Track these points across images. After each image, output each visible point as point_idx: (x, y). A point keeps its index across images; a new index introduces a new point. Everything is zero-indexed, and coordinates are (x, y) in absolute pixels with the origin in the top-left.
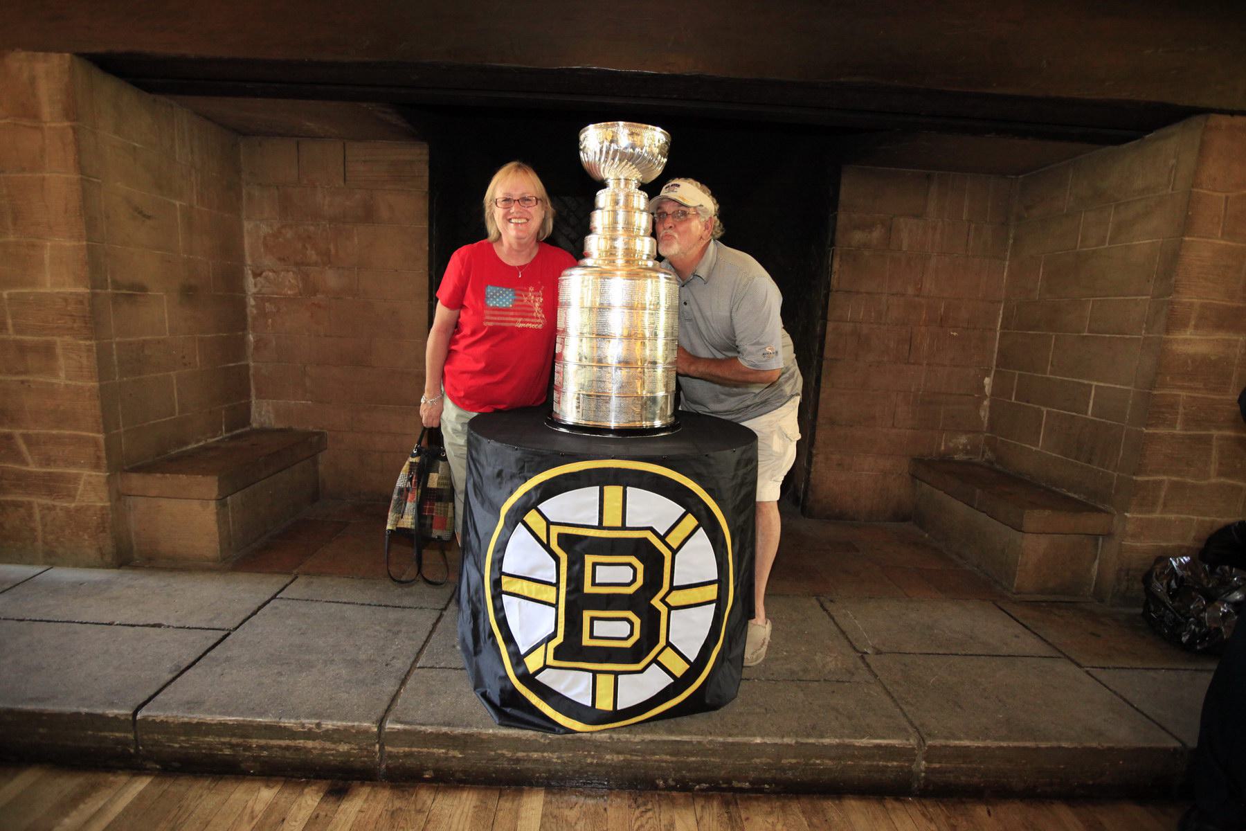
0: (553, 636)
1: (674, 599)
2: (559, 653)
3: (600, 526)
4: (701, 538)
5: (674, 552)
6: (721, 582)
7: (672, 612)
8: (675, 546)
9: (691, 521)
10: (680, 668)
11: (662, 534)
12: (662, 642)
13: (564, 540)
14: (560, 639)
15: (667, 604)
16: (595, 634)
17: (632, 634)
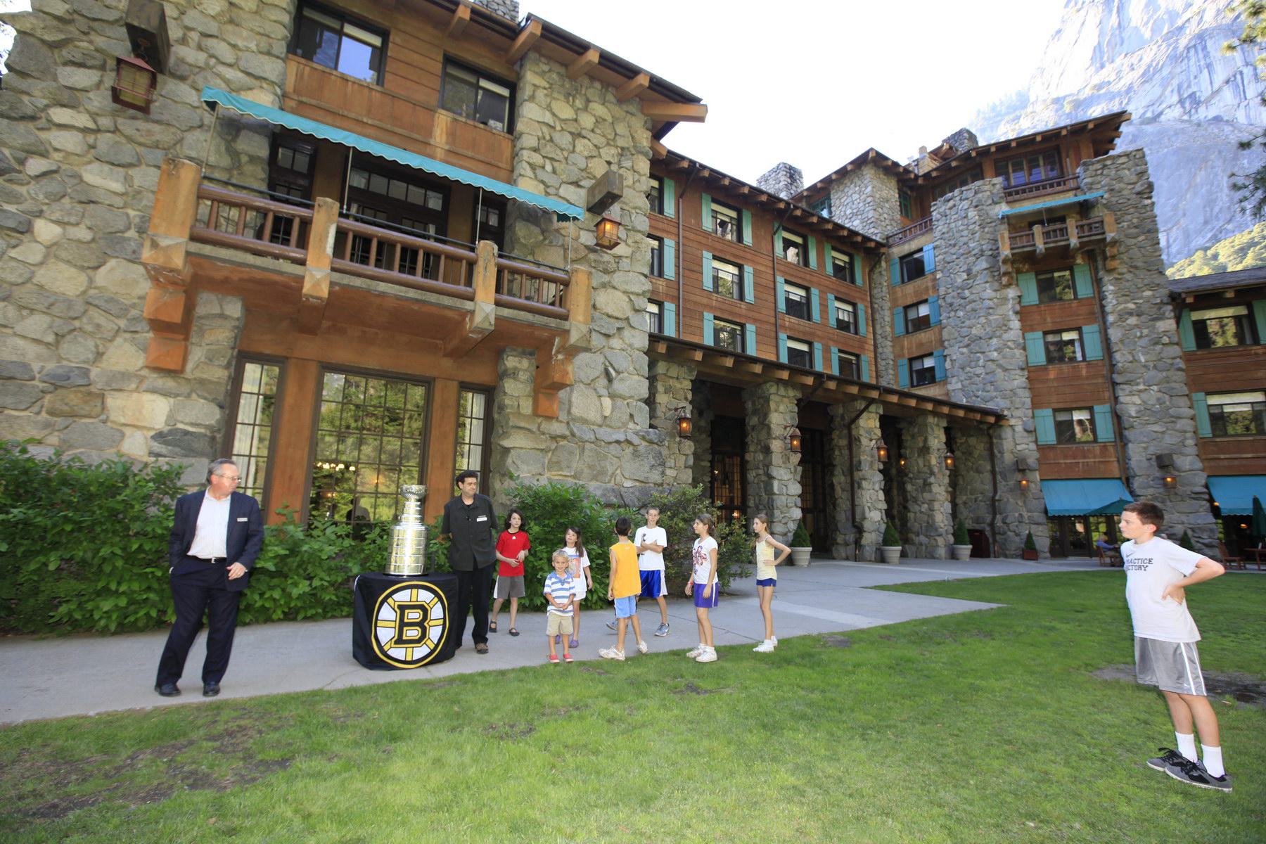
1: (431, 623)
2: (396, 643)
4: (439, 605)
6: (444, 618)
9: (436, 599)
10: (432, 646)
13: (400, 607)
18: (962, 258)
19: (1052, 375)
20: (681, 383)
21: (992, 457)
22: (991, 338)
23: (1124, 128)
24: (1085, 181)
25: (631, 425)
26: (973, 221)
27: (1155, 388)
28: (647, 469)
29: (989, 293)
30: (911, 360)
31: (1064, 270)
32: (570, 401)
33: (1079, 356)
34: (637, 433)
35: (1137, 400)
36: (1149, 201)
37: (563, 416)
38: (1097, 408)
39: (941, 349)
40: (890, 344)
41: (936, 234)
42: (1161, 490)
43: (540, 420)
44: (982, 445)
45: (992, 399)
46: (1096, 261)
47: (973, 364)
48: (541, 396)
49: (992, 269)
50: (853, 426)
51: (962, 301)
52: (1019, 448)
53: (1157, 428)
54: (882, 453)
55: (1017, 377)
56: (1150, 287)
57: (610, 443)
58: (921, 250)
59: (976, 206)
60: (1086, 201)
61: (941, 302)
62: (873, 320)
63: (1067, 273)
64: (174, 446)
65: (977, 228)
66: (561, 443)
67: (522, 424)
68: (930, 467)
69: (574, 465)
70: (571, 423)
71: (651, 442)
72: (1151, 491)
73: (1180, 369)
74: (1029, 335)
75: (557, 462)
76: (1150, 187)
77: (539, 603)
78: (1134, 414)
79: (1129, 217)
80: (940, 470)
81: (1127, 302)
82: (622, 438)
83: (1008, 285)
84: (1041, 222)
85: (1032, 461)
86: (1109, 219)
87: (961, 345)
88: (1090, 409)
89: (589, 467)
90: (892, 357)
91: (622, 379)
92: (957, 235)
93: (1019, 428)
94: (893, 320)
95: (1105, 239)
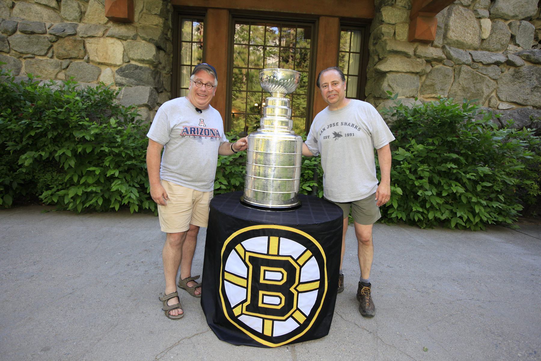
0: (245, 301)
1: (301, 288)
2: (248, 308)
3: (268, 254)
4: (314, 261)
5: (301, 267)
7: (299, 294)
8: (301, 264)
9: (309, 253)
10: (302, 319)
11: (295, 259)
12: (295, 308)
14: (248, 302)
15: (297, 290)
16: (264, 302)
17: (281, 303)
20: (533, 24)
25: (511, 47)
28: (528, 91)
32: (447, 25)
34: (519, 55)
37: (439, 41)
43: (416, 45)
48: (419, 20)
57: (489, 65)
64: (130, 78)
66: (436, 67)
67: (400, 48)
69: (448, 87)
70: (447, 47)
71: (536, 63)
75: (432, 85)
77: (416, 219)
82: (502, 59)
89: (464, 90)
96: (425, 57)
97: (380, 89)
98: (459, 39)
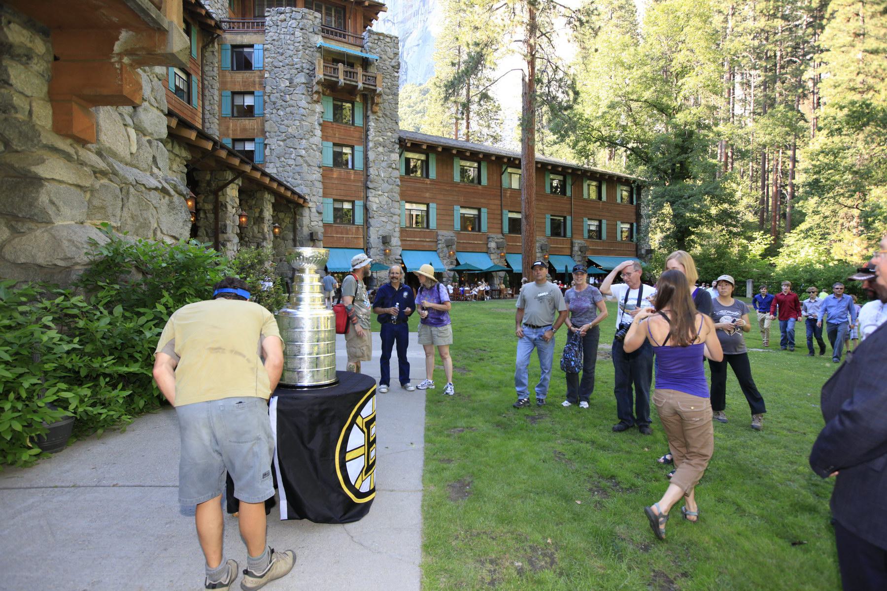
18: (287, 67)
19: (335, 175)
21: (294, 230)
22: (301, 139)
23: (381, 15)
24: (369, 44)
25: (155, 170)
26: (298, 40)
27: (386, 194)
29: (303, 103)
30: (235, 141)
31: (347, 102)
33: (350, 166)
35: (377, 200)
36: (396, 74)
38: (357, 202)
39: (262, 138)
40: (217, 122)
41: (267, 38)
42: (383, 257)
43: (69, 141)
44: (289, 219)
45: (298, 185)
46: (367, 104)
47: (287, 156)
49: (308, 85)
50: (220, 193)
51: (283, 103)
52: (313, 224)
53: (384, 219)
54: (244, 219)
55: (316, 172)
56: (393, 131)
57: (150, 189)
58: (252, 46)
59: (302, 29)
60: (367, 58)
61: (266, 98)
62: (203, 95)
63: (349, 105)
65: (301, 47)
68: (263, 234)
72: (378, 257)
73: (398, 185)
74: (325, 143)
76: (399, 64)
78: (375, 209)
79: (386, 80)
80: (269, 234)
81: (379, 136)
83: (317, 102)
84: (344, 63)
85: (320, 235)
86: (379, 78)
87: (279, 138)
88: (353, 202)
90: (217, 133)
91: (145, 110)
92: (284, 46)
93: (314, 210)
94: (220, 100)
95: (376, 90)
96: (92, 166)
97: (31, 205)
98: (112, 147)
